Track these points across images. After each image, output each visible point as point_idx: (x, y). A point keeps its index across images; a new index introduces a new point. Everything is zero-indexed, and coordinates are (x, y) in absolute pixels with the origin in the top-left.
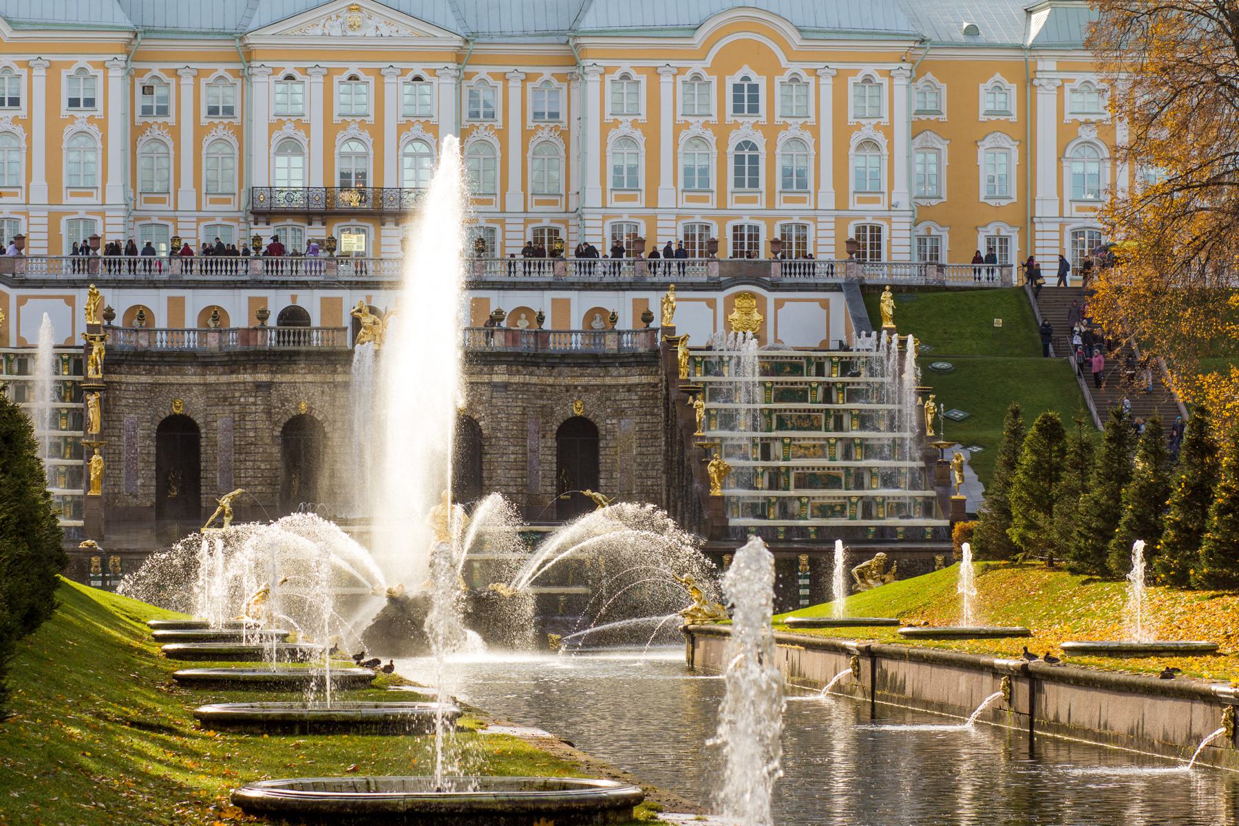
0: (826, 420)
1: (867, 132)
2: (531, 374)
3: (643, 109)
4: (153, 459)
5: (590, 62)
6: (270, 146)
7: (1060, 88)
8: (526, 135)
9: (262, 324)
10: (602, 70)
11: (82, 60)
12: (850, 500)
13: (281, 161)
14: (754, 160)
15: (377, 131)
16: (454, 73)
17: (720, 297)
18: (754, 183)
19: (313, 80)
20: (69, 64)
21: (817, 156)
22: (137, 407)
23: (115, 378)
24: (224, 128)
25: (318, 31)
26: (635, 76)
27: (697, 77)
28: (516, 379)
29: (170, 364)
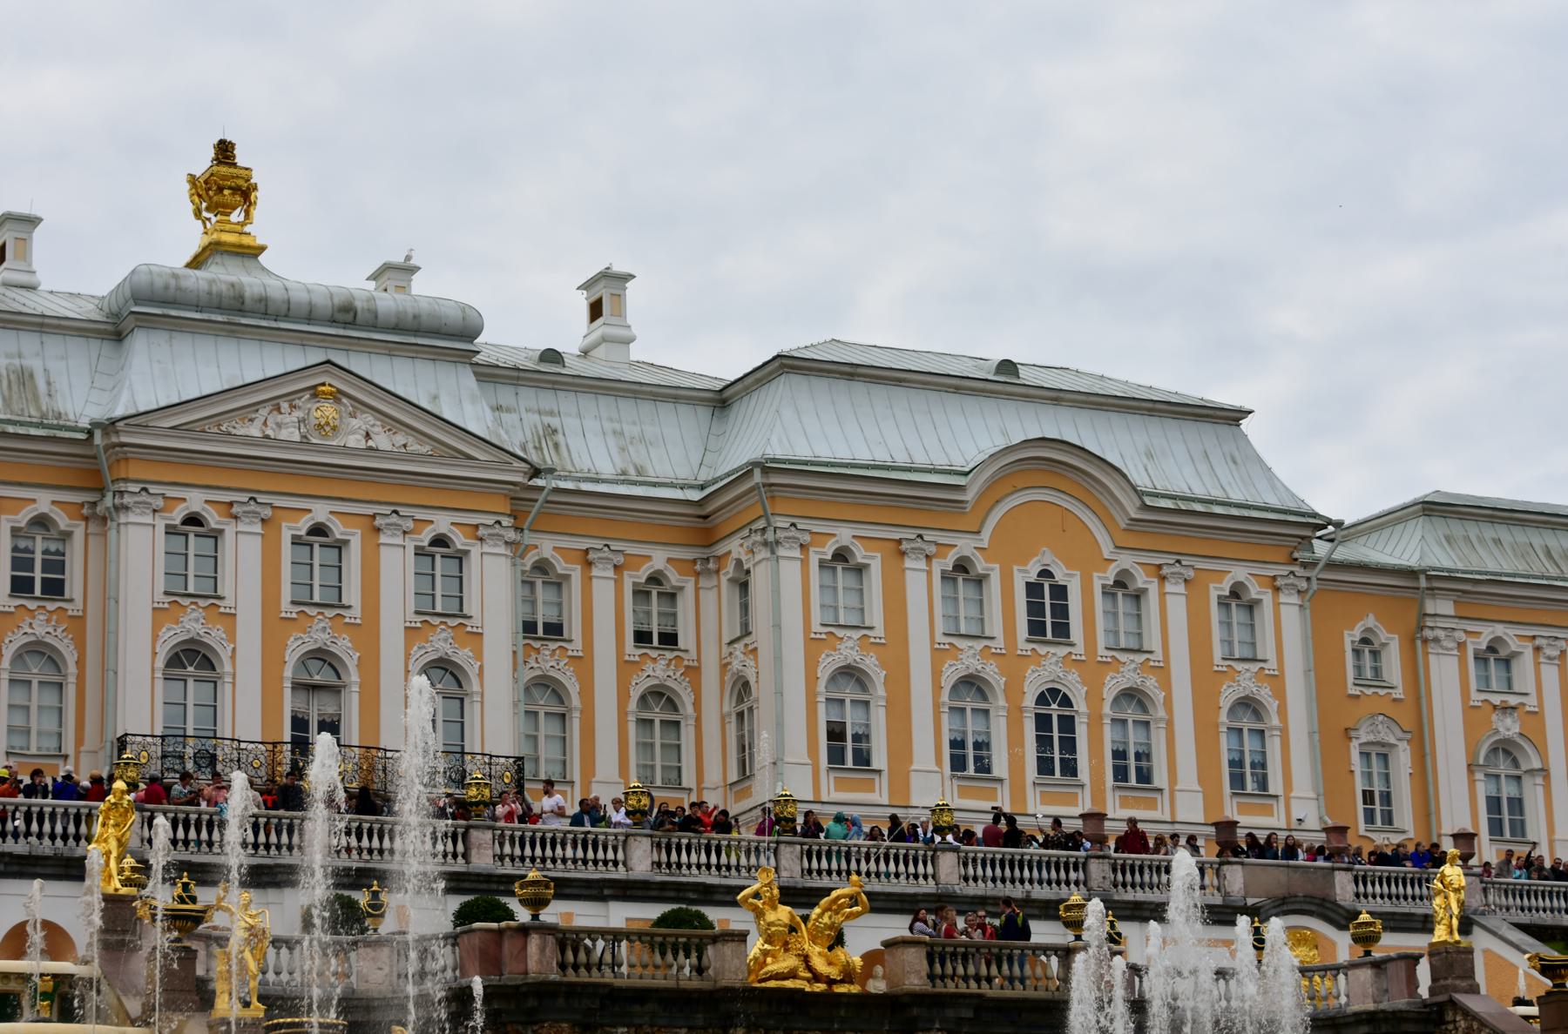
1: (1246, 682)
3: (876, 616)
5: (782, 522)
6: (155, 654)
7: (1461, 646)
8: (625, 668)
9: (535, 917)
14: (1068, 723)
15: (367, 632)
18: (1070, 768)
19: (241, 528)
21: (1170, 724)
24: (48, 621)
25: (254, 431)
26: (860, 554)
27: (962, 566)
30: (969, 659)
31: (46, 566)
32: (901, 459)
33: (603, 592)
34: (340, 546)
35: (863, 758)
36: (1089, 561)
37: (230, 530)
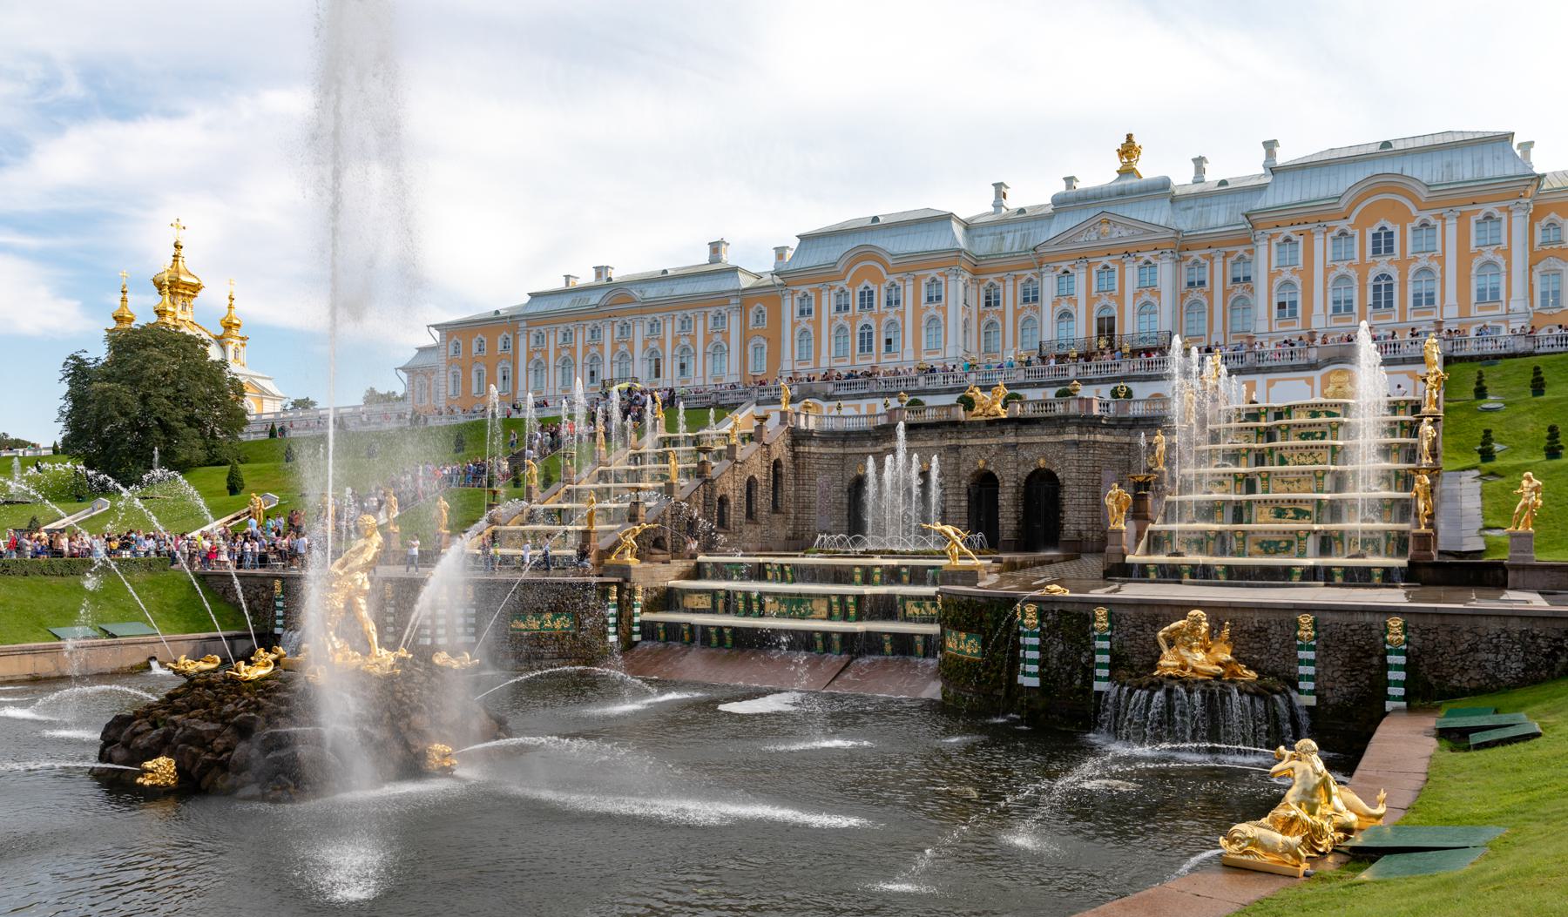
0: (1332, 456)
1: (1489, 255)
2: (1107, 434)
3: (1300, 261)
4: (845, 506)
5: (1259, 232)
8: (1226, 292)
10: (1269, 236)
11: (933, 273)
12: (1297, 535)
13: (1063, 325)
14: (1389, 287)
15: (1120, 299)
16: (1170, 255)
17: (1317, 375)
18: (1389, 304)
20: (925, 276)
22: (833, 470)
23: (802, 449)
25: (1082, 240)
26: (1294, 238)
28: (1086, 437)
29: (855, 440)
30: (1342, 269)
31: (1033, 293)
32: (1312, 198)
33: (1218, 266)
34: (1113, 270)
35: (1293, 314)
36: (1404, 217)
37: (1076, 272)
